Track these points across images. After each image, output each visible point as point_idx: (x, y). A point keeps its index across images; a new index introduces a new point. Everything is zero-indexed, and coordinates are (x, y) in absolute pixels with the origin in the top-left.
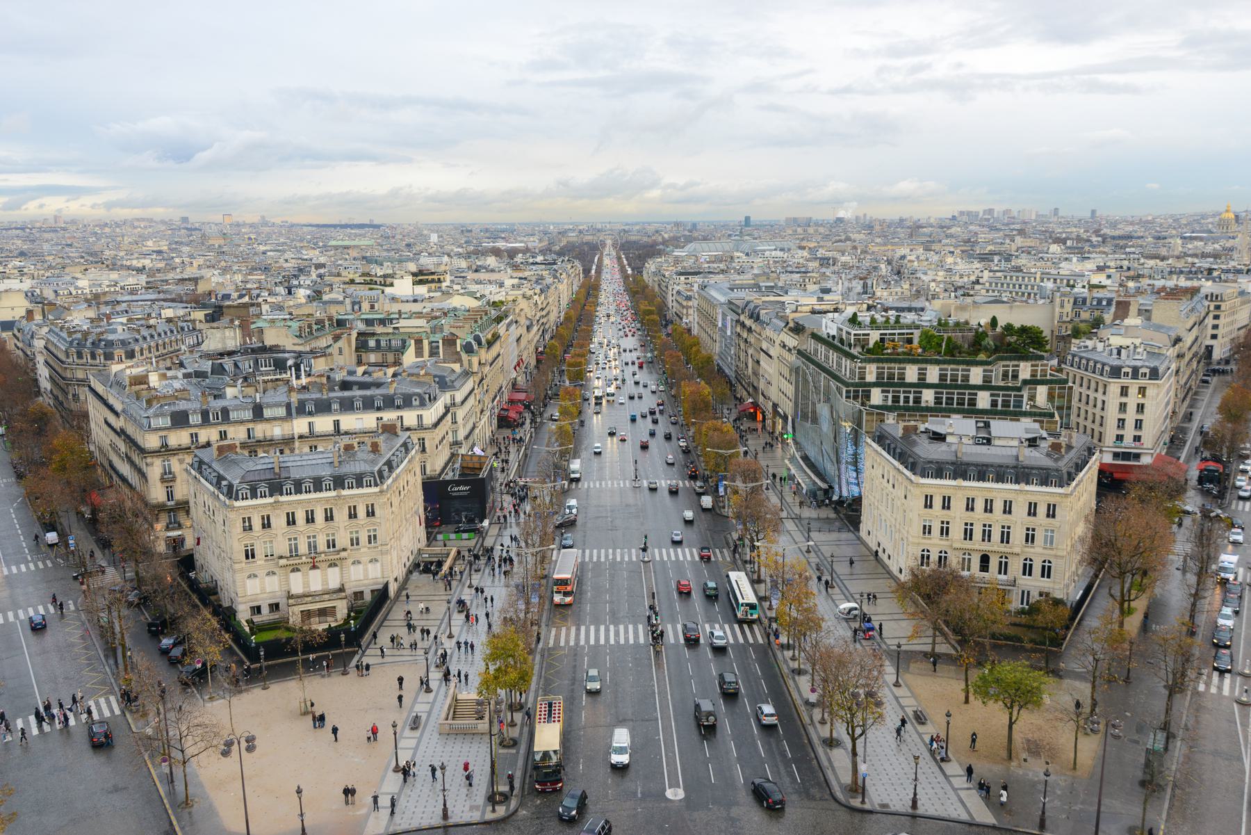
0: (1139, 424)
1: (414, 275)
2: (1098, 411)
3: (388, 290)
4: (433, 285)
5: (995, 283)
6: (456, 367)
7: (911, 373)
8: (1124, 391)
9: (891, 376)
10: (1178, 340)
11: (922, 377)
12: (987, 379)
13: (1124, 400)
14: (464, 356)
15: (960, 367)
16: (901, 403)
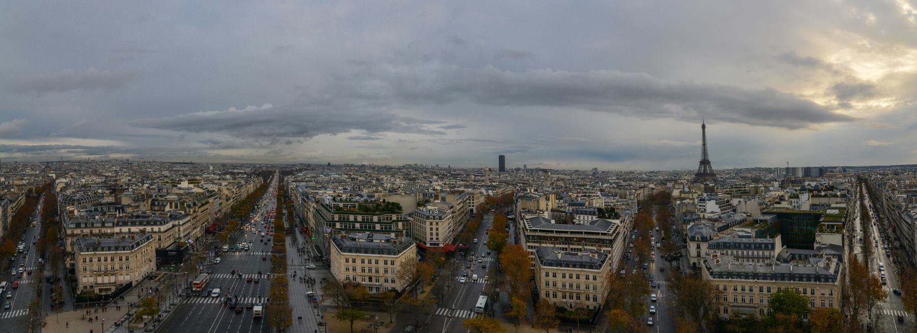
0: (437, 234)
1: (189, 180)
2: (424, 230)
3: (179, 186)
4: (196, 184)
5: (404, 187)
6: (183, 212)
7: (352, 218)
8: (431, 224)
9: (344, 218)
10: (452, 207)
11: (356, 219)
12: (379, 220)
13: (431, 226)
14: (187, 209)
15: (369, 216)
16: (348, 228)
